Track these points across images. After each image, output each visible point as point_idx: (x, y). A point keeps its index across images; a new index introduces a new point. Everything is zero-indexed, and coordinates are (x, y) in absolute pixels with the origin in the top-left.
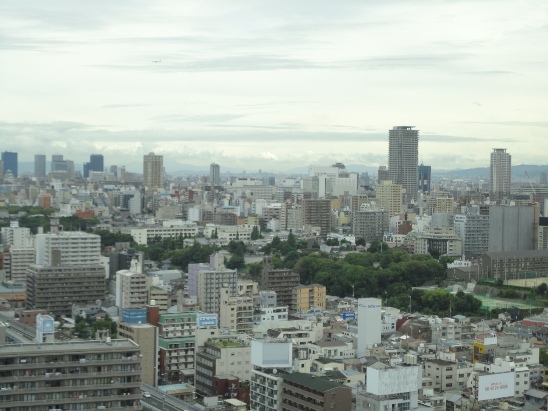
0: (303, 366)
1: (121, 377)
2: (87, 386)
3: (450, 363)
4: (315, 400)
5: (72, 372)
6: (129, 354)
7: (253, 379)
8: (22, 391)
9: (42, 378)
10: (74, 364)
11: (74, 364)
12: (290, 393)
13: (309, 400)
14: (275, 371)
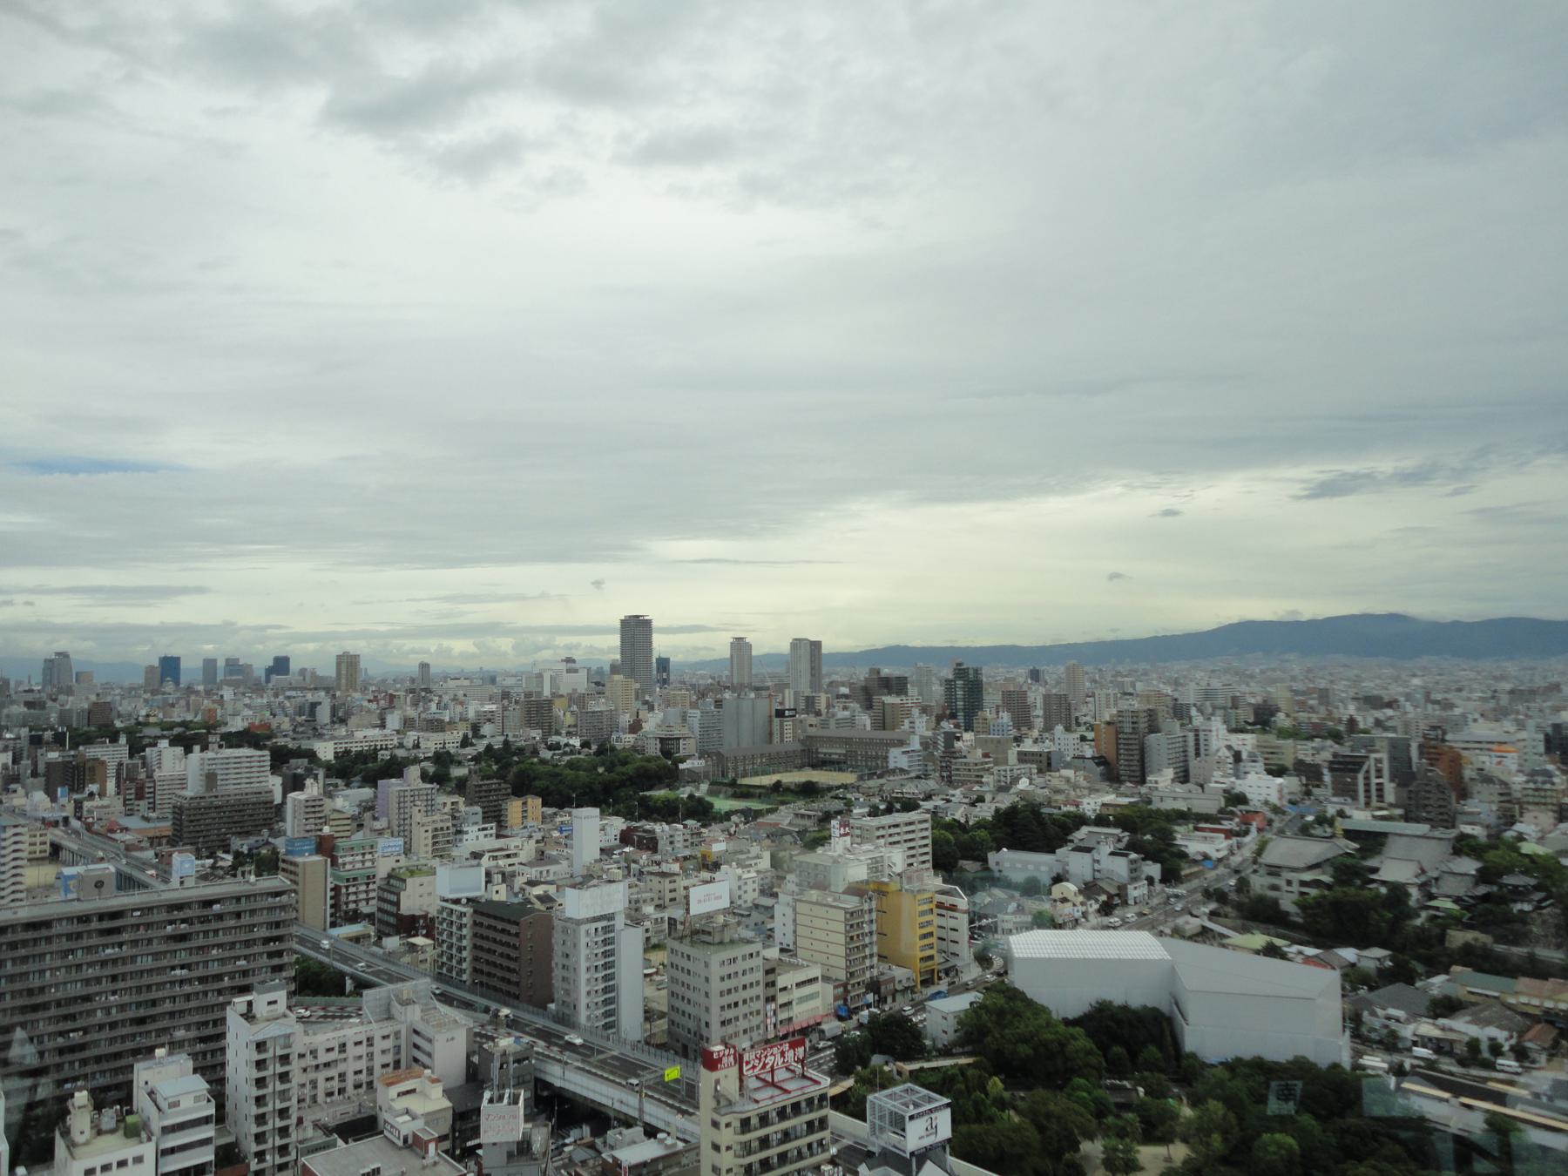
0: (497, 892)
1: (268, 923)
2: (222, 938)
3: (675, 874)
5: (202, 923)
6: (278, 894)
8: (134, 951)
9: (162, 933)
10: (206, 912)
11: (206, 912)
13: (503, 931)
14: (464, 901)
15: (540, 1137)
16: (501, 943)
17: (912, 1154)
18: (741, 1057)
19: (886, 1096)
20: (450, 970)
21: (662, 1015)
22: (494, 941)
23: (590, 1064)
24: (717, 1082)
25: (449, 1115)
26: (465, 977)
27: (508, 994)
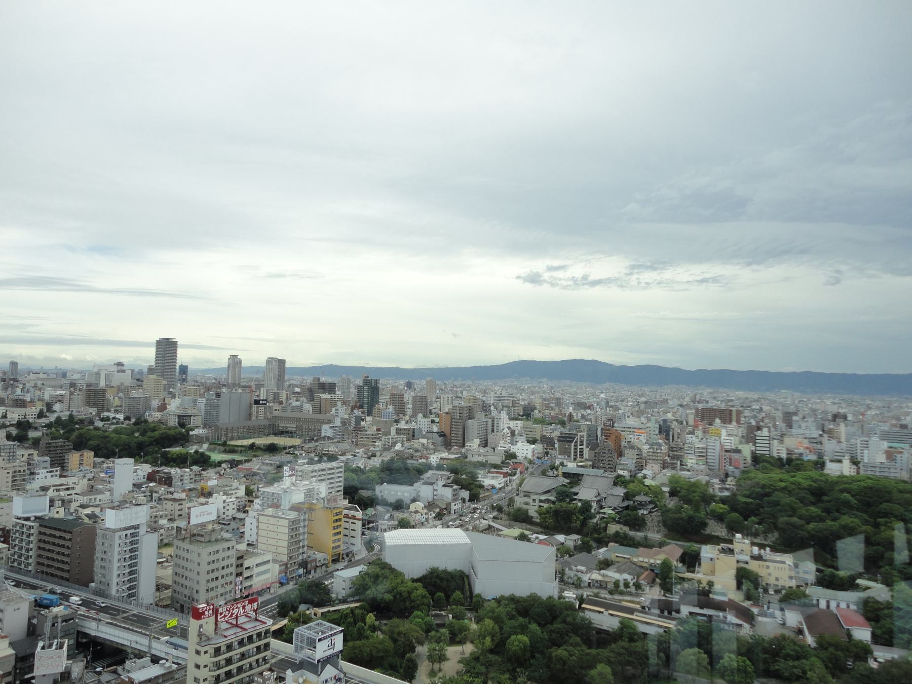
0: (57, 512)
3: (182, 500)
4: (64, 537)
7: (14, 526)
12: (45, 534)
13: (60, 537)
14: (33, 519)
15: (77, 668)
16: (58, 545)
17: (319, 661)
18: (217, 610)
19: (305, 629)
20: (20, 564)
21: (167, 587)
22: (54, 544)
23: (117, 620)
24: (201, 626)
25: (13, 659)
26: (30, 568)
27: (62, 578)
